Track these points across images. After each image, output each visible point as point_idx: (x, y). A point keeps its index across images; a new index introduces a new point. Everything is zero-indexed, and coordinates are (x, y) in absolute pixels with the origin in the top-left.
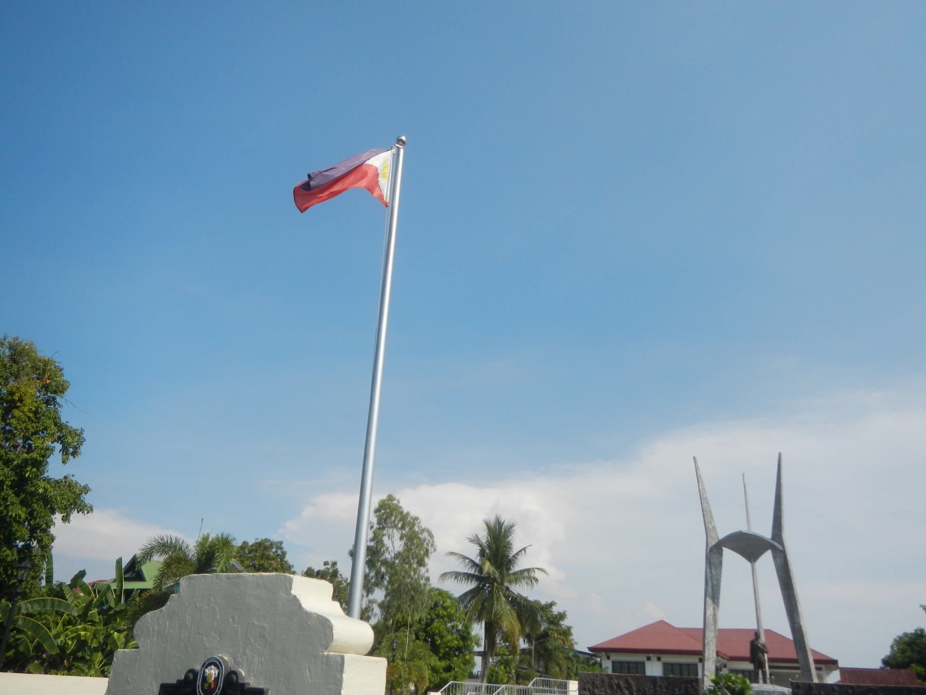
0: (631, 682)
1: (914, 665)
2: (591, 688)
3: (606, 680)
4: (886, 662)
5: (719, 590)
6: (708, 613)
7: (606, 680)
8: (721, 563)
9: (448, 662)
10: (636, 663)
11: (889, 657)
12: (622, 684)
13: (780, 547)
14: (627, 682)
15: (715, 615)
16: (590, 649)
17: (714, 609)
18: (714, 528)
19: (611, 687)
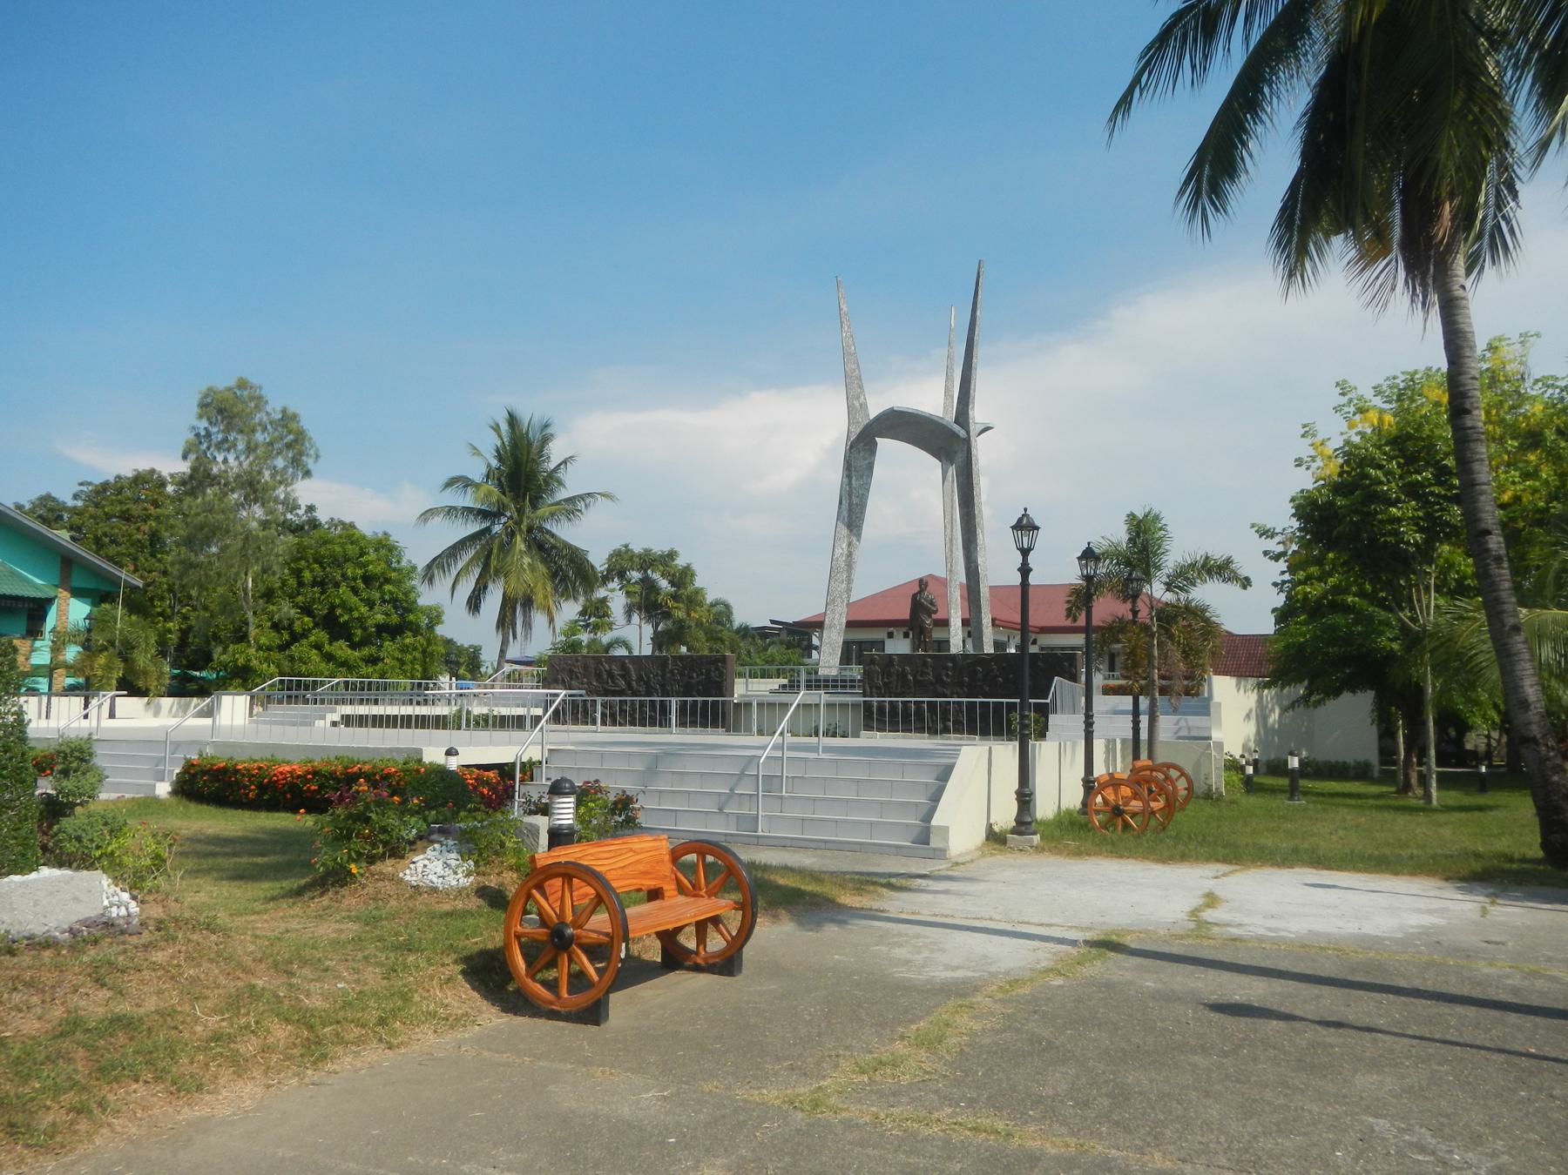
2: (567, 679)
3: (591, 663)
5: (863, 512)
6: (838, 551)
7: (591, 663)
8: (870, 467)
9: (373, 649)
12: (616, 671)
13: (962, 433)
14: (623, 667)
15: (850, 555)
17: (850, 544)
18: (864, 406)
19: (599, 676)
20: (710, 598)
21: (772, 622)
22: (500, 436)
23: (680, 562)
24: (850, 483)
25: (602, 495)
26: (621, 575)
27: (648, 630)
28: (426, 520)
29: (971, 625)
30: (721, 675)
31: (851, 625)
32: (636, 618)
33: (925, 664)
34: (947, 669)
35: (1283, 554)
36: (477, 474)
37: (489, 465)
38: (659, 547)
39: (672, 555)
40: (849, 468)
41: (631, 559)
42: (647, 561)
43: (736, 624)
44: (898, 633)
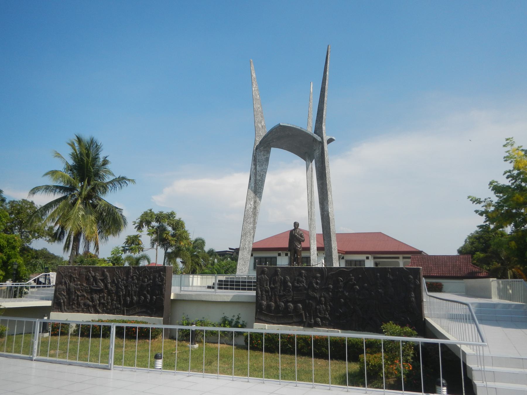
0: (108, 274)
1: (478, 253)
2: (68, 281)
4: (459, 251)
7: (83, 271)
8: (267, 160)
10: (271, 258)
11: (462, 248)
13: (319, 139)
14: (103, 274)
15: (255, 208)
17: (255, 202)
19: (88, 280)
20: (193, 237)
21: (230, 249)
22: (75, 150)
23: (177, 218)
24: (255, 169)
25: (129, 180)
26: (148, 223)
27: (161, 252)
28: (34, 193)
29: (325, 249)
30: (162, 280)
31: (254, 250)
32: (155, 246)
33: (300, 275)
34: (316, 278)
35: (486, 212)
36: (60, 167)
37: (67, 163)
38: (166, 211)
39: (172, 214)
40: (255, 160)
41: (151, 216)
42: (160, 218)
43: (207, 249)
44: (283, 254)
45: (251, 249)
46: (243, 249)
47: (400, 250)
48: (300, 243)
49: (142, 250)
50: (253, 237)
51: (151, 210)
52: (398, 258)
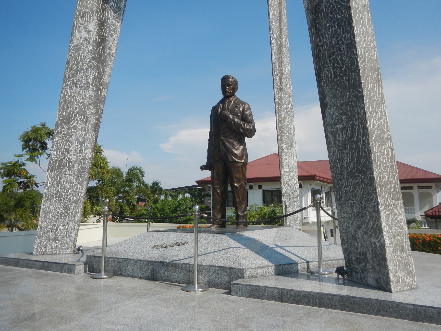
15: (102, 41)
16: (198, 182)
17: (102, 24)
45: (88, 165)
46: (61, 166)
47: (415, 177)
48: (242, 142)
49: (36, 185)
50: (96, 128)
51: (43, 125)
52: (411, 188)
